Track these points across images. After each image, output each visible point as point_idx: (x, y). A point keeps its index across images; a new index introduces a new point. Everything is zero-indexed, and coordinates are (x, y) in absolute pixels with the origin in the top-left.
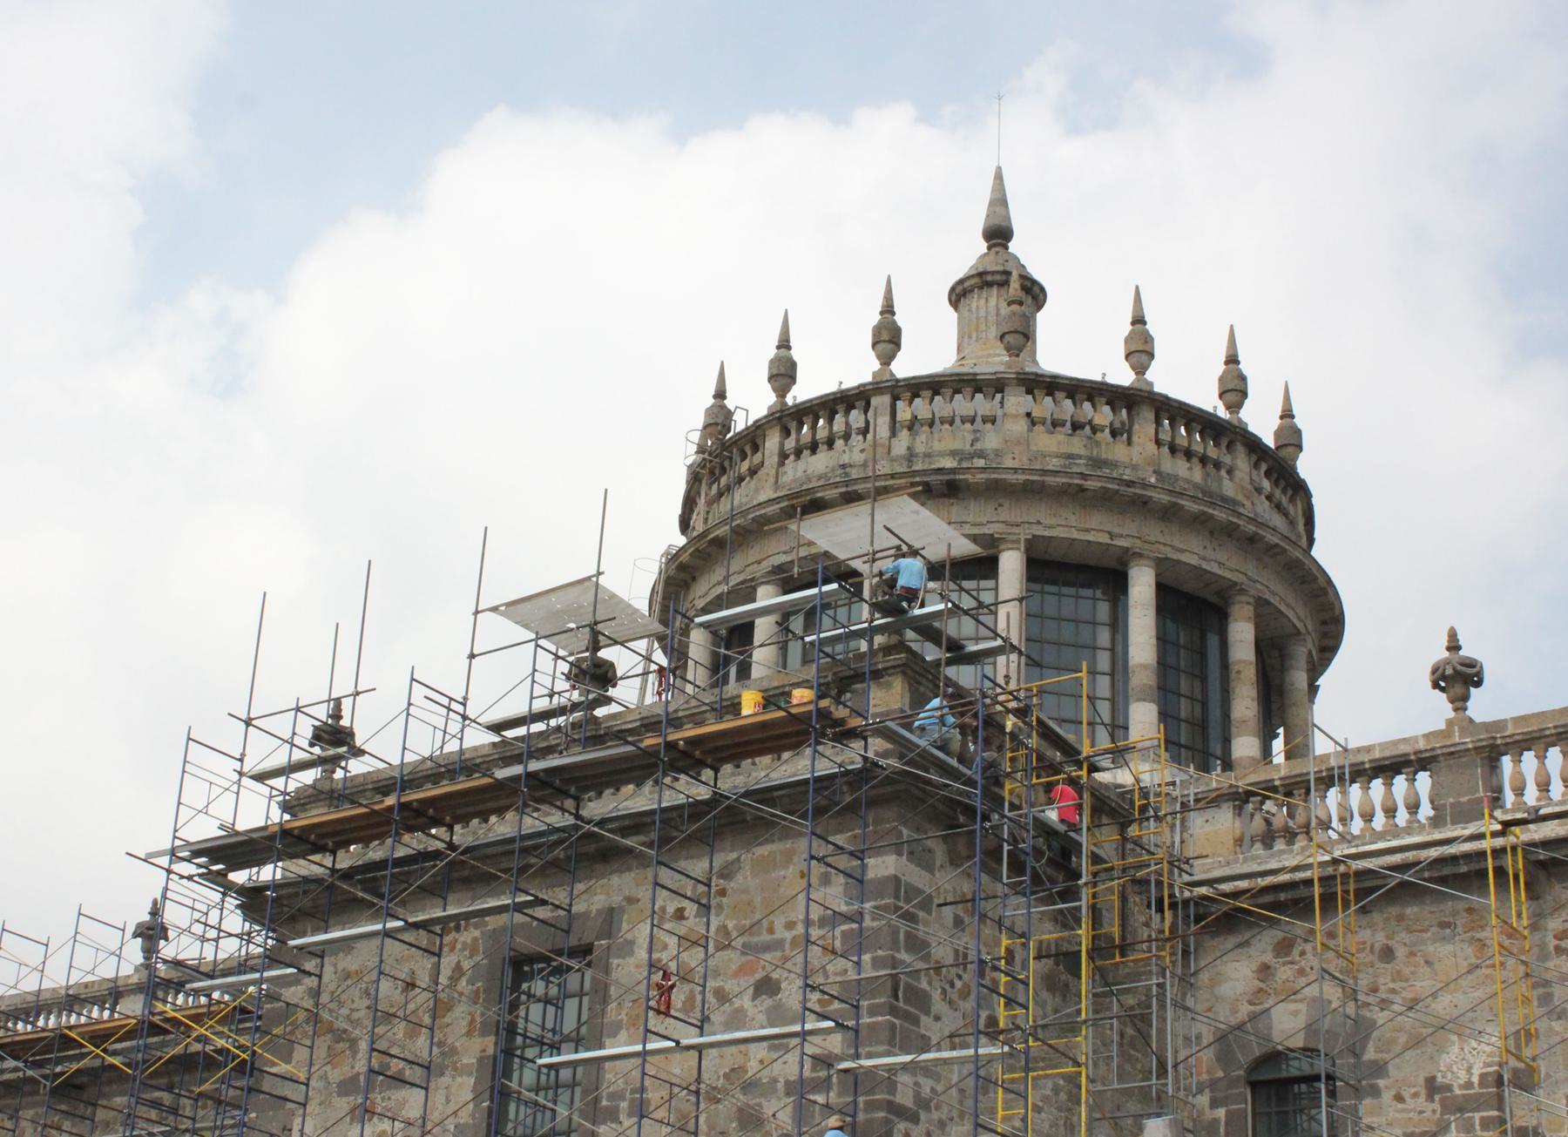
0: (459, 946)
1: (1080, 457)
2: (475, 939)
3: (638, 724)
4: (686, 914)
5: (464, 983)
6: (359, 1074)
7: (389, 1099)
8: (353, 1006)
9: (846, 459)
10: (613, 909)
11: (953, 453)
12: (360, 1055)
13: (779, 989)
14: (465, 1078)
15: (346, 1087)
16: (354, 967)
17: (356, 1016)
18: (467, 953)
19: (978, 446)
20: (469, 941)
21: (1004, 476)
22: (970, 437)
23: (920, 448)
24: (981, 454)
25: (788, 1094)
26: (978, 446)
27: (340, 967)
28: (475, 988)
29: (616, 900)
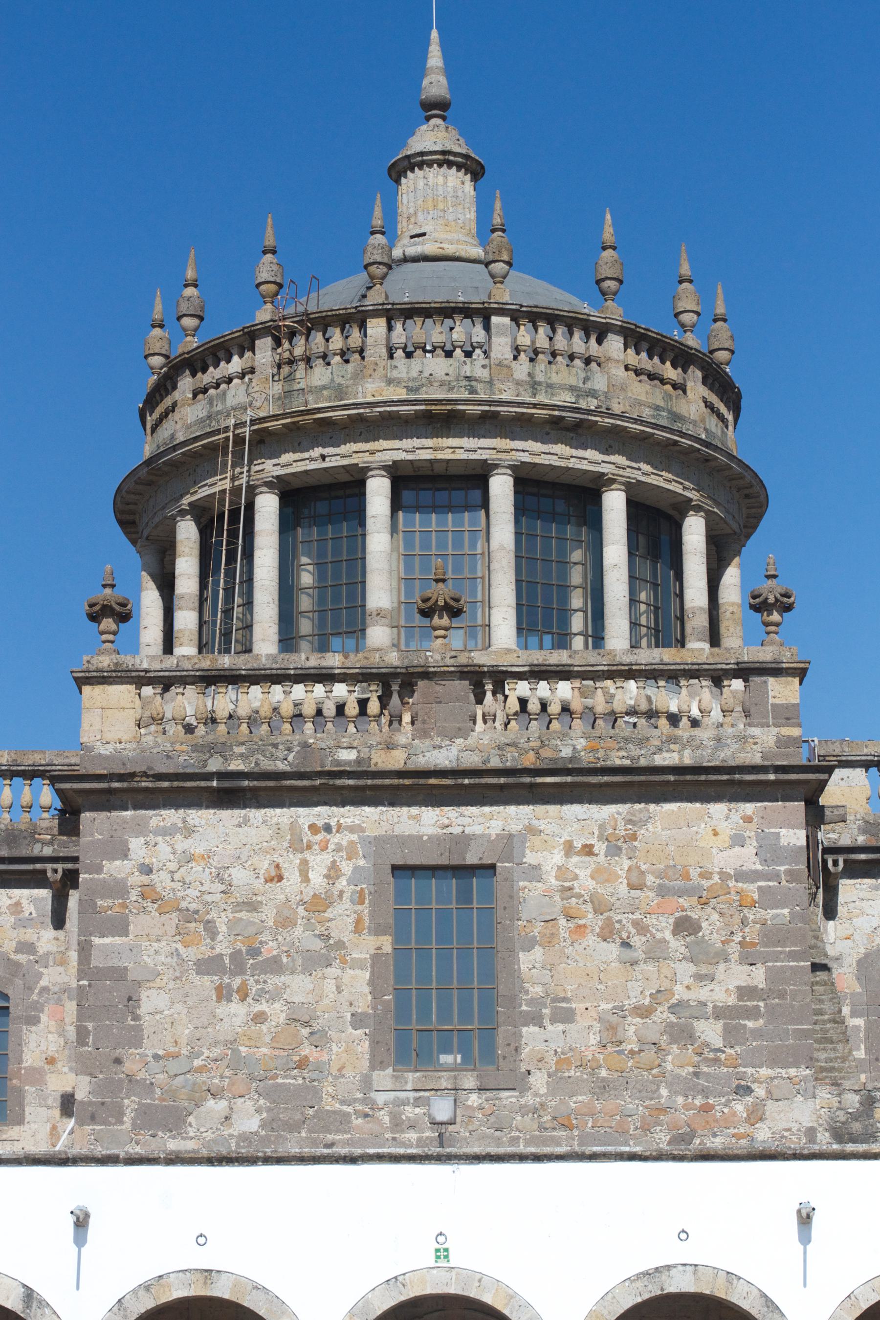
0: (331, 847)
1: (663, 409)
2: (352, 842)
3: (526, 669)
4: (596, 850)
5: (345, 883)
6: (221, 956)
7: (265, 982)
8: (203, 889)
9: (467, 370)
10: (511, 836)
11: (572, 389)
12: (220, 937)
13: (700, 928)
14: (358, 972)
15: (207, 966)
16: (199, 850)
17: (209, 898)
18: (344, 854)
19: (589, 385)
20: (344, 843)
21: (626, 424)
22: (582, 375)
23: (540, 377)
24: (593, 394)
25: (717, 1017)
26: (589, 385)
27: (180, 847)
28: (358, 888)
29: (515, 827)
